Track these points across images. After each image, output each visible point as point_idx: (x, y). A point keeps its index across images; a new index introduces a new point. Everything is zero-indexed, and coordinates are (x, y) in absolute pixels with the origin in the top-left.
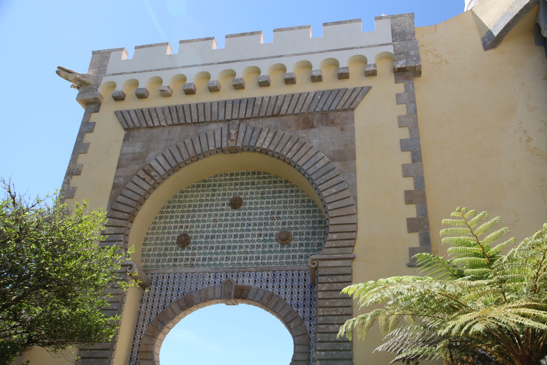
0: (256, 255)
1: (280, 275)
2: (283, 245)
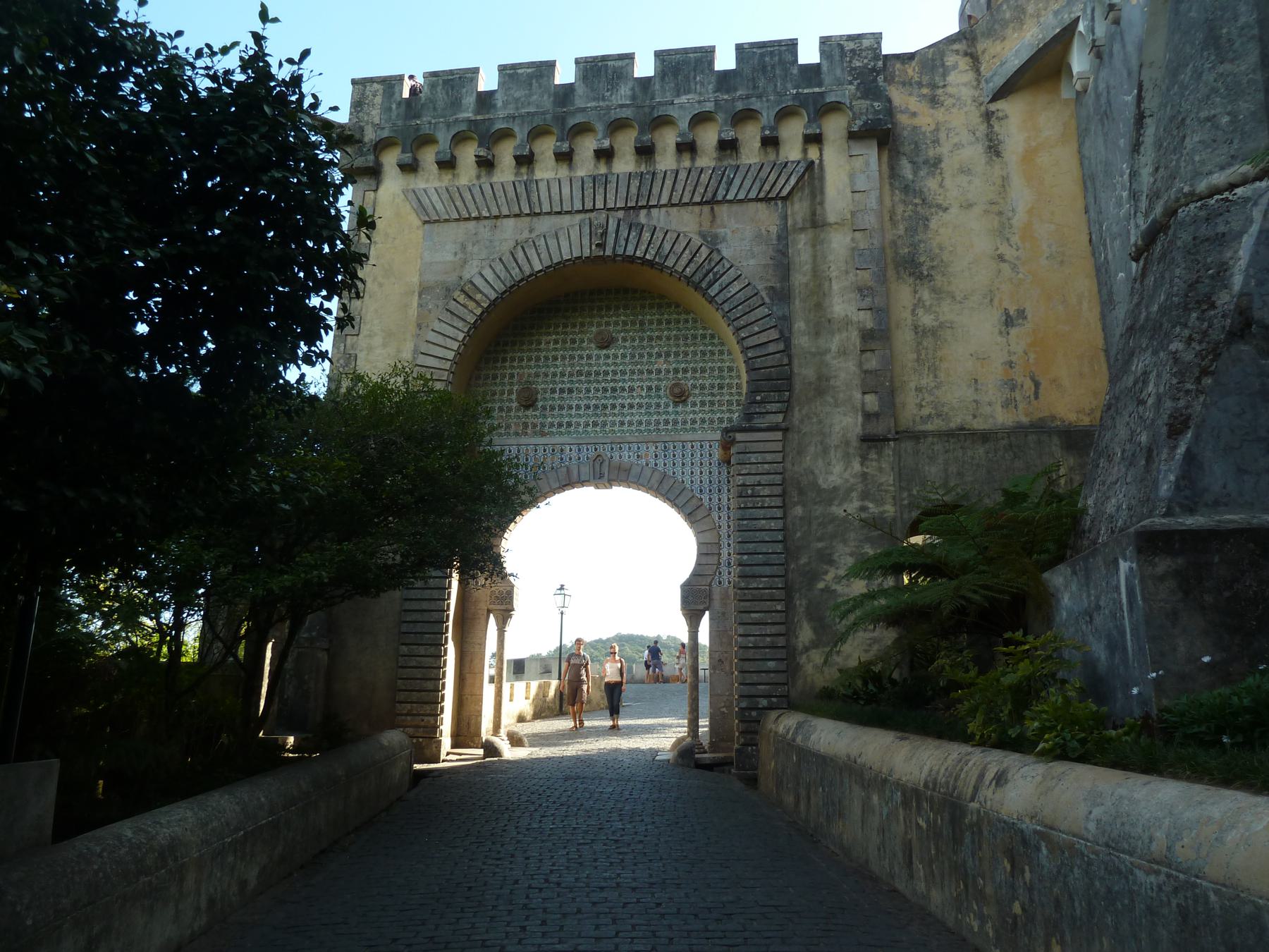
1: (674, 447)
2: (676, 404)
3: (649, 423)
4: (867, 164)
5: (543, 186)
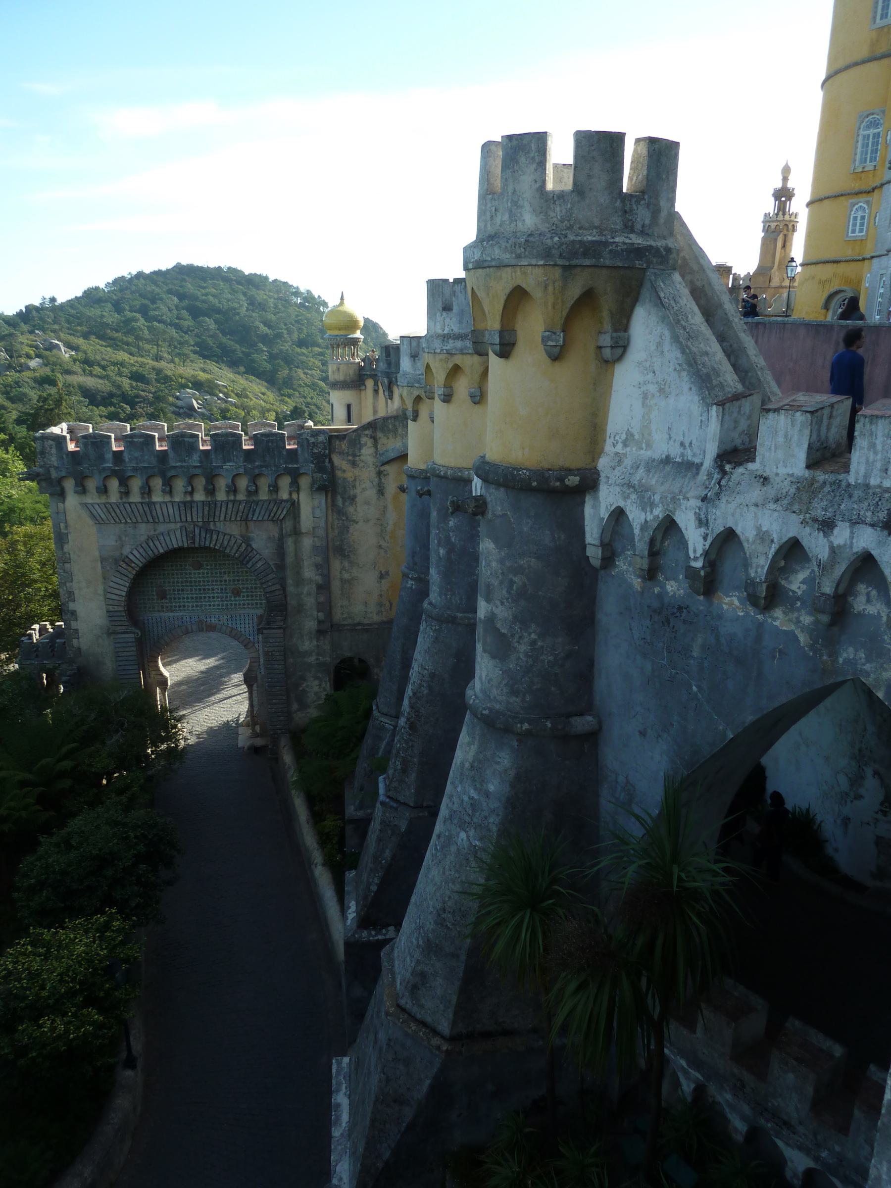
0: (217, 603)
3: (223, 605)
4: (320, 503)
5: (158, 506)
